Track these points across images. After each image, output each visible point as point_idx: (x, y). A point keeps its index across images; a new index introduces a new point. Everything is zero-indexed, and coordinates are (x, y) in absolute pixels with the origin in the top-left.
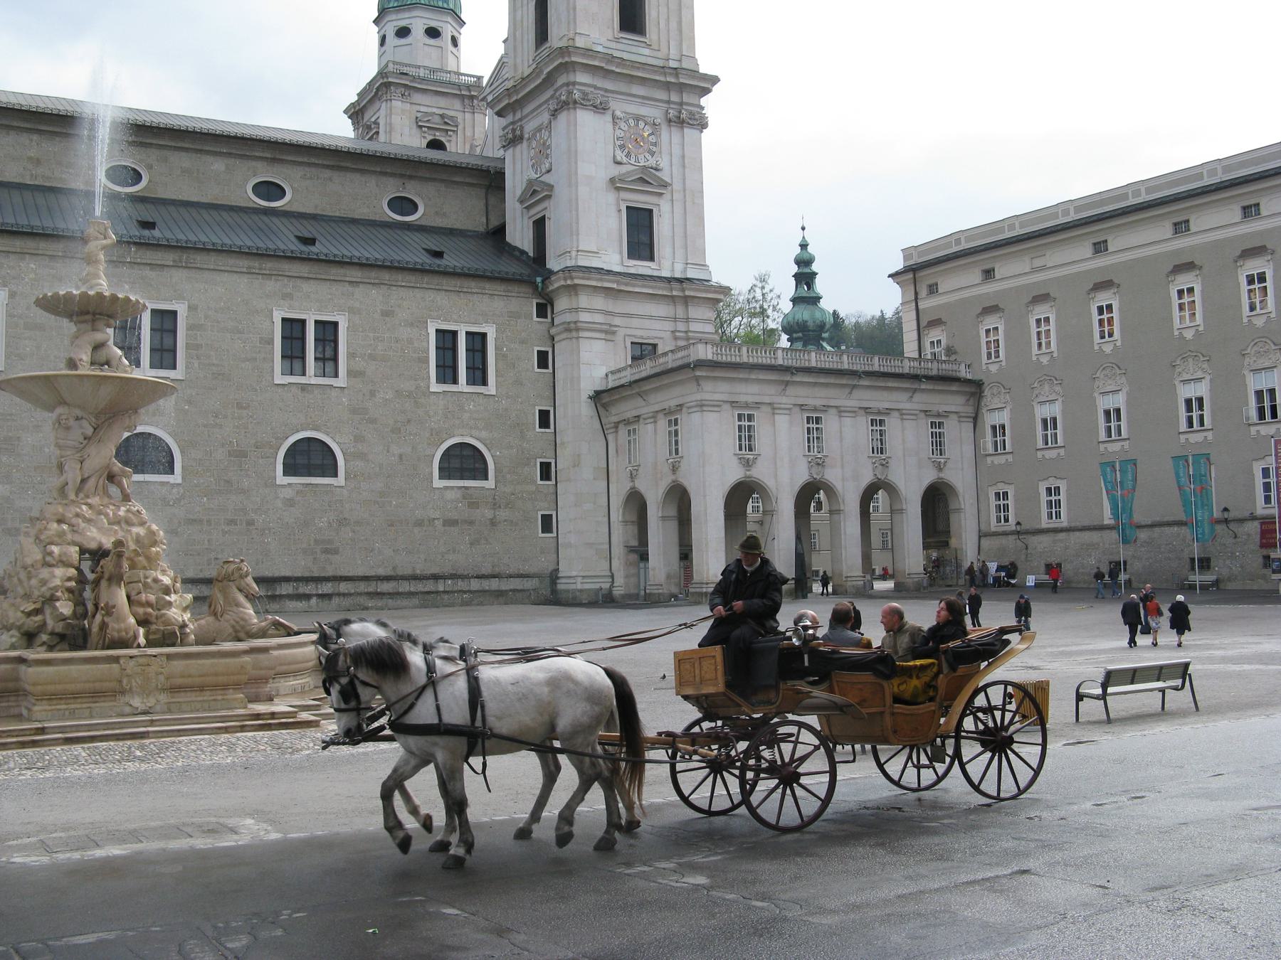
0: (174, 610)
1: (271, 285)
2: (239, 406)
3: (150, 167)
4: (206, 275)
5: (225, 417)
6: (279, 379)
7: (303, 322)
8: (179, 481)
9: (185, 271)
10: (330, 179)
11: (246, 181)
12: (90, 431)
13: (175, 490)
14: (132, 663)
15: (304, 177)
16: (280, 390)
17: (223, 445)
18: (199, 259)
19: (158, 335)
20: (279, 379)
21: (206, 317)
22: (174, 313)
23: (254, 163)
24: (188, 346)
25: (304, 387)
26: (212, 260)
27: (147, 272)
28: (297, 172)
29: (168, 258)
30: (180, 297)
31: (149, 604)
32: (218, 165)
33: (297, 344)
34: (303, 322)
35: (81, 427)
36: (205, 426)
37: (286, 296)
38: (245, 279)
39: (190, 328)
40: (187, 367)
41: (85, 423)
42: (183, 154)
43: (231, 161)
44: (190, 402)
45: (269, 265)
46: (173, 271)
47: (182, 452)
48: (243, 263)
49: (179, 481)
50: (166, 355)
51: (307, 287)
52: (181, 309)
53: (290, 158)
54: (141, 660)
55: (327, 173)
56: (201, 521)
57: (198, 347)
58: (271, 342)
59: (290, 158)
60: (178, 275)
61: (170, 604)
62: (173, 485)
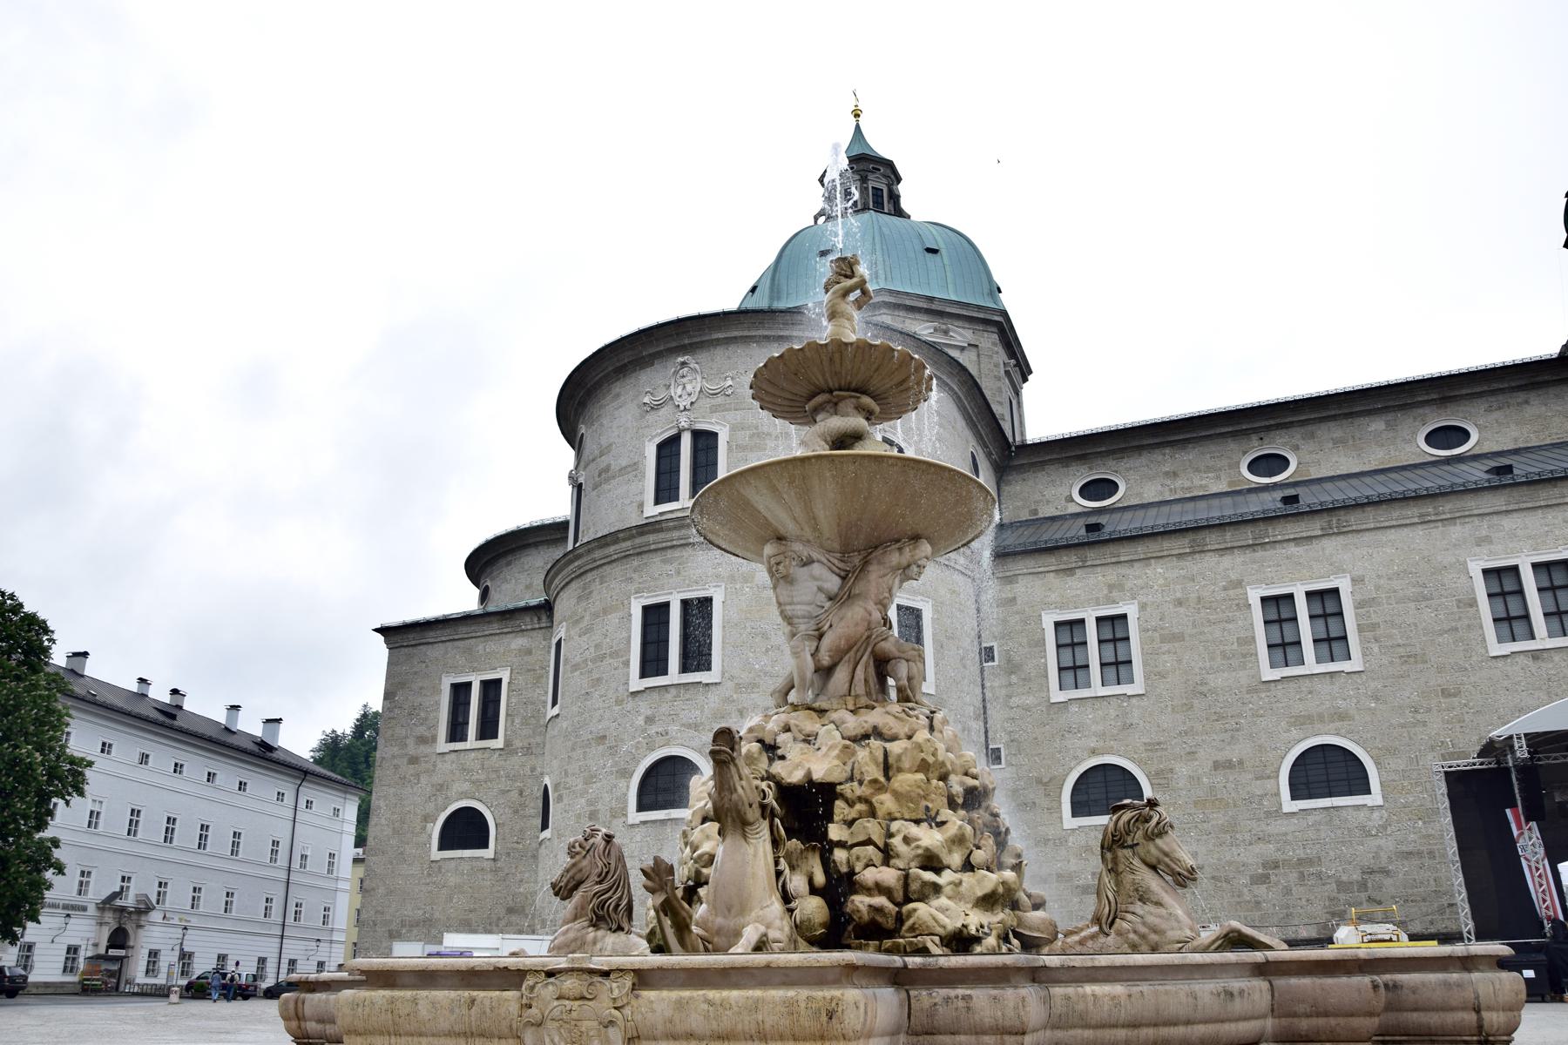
0: (943, 901)
1: (1457, 531)
2: (1445, 693)
3: (1296, 448)
4: (1367, 537)
5: (1429, 710)
6: (1497, 649)
7: (1514, 570)
8: (1380, 802)
9: (1341, 539)
10: (1527, 402)
11: (1415, 433)
12: (833, 583)
13: (1376, 815)
14: (547, 991)
15: (1489, 410)
16: (1500, 664)
17: (1432, 748)
18: (1354, 519)
19: (1320, 623)
20: (1497, 649)
21: (1378, 588)
22: (1336, 591)
23: (1420, 411)
24: (1360, 629)
25: (1536, 655)
26: (1370, 517)
27: (1293, 549)
28: (1480, 406)
29: (1314, 527)
30: (1339, 570)
31: (880, 889)
32: (1377, 425)
33: (1513, 603)
34: (1514, 570)
35: (815, 579)
36: (1403, 726)
37: (1480, 542)
38: (1420, 532)
39: (1359, 605)
40: (1364, 655)
41: (816, 569)
42: (1332, 424)
43: (1390, 416)
44: (1377, 699)
45: (1447, 507)
46: (1326, 542)
47: (1377, 763)
48: (1412, 512)
49: (1380, 802)
50: (1335, 645)
51: (1508, 523)
52: (1344, 585)
53: (1464, 392)
54: (570, 984)
55: (1521, 396)
56: (1419, 854)
57: (1374, 626)
58: (1473, 603)
59: (1464, 392)
60: (1330, 545)
61: (937, 889)
62: (1372, 809)
